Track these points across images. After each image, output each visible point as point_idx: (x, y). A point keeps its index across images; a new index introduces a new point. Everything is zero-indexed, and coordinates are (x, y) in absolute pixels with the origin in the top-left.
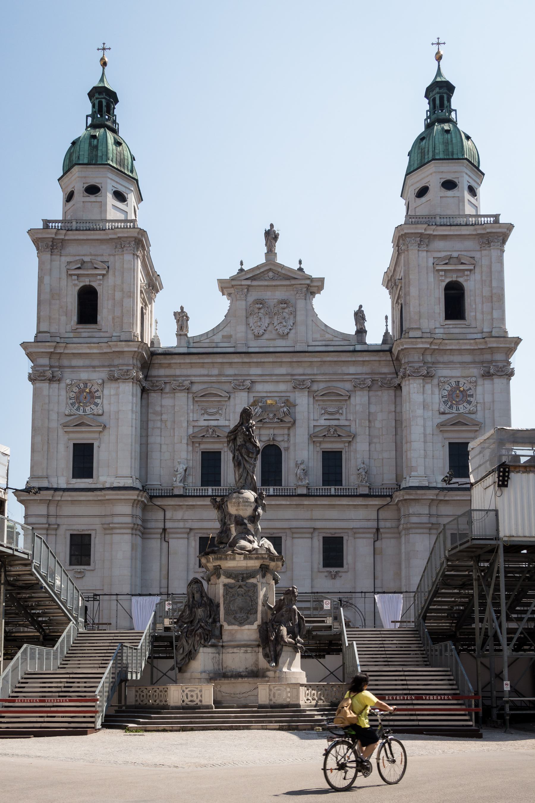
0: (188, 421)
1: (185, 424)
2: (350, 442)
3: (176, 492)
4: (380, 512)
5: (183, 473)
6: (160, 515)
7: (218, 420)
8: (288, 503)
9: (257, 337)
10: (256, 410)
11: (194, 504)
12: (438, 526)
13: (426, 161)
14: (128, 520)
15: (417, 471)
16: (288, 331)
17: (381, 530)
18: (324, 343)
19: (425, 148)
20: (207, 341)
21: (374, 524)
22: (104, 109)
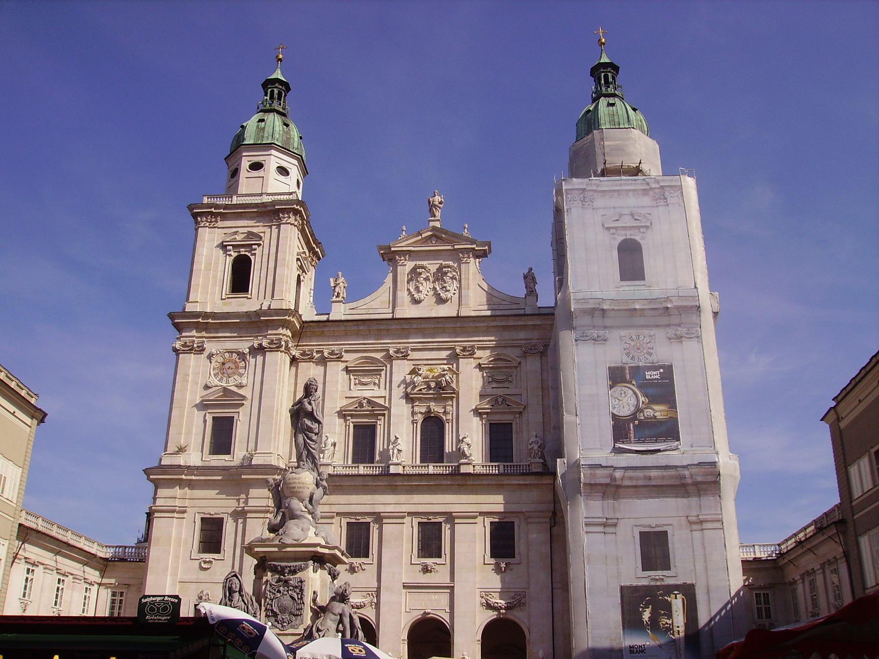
2: (521, 413)
7: (373, 390)
8: (449, 483)
9: (416, 302)
10: (415, 379)
11: (342, 484)
16: (452, 295)
19: (591, 119)
22: (276, 96)
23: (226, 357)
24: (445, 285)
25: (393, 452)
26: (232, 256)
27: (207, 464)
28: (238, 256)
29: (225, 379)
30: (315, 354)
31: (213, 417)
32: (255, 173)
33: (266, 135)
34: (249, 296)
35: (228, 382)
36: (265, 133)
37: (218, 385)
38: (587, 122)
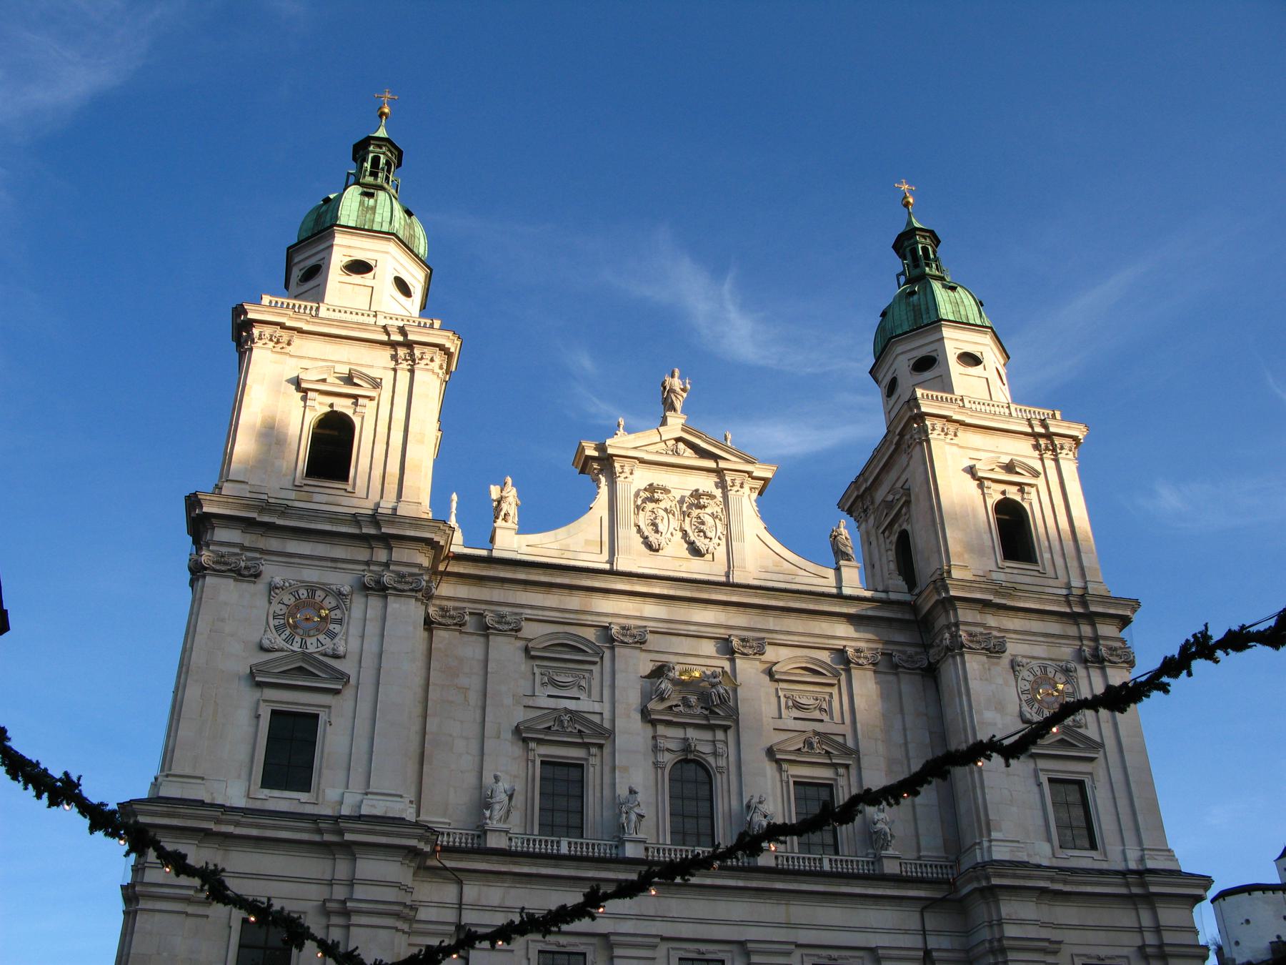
0: (513, 696)
1: (508, 701)
3: (493, 842)
4: (926, 915)
5: (507, 798)
6: (448, 892)
7: (579, 699)
8: (741, 883)
10: (663, 686)
12: (1056, 946)
13: (925, 322)
14: (390, 894)
15: (1000, 830)
17: (934, 954)
18: (781, 577)
19: (920, 305)
20: (555, 546)
21: (916, 941)
23: (301, 597)
24: (702, 527)
25: (629, 821)
26: (315, 410)
27: (257, 805)
28: (331, 411)
29: (298, 639)
30: (467, 618)
31: (272, 710)
32: (356, 278)
33: (378, 219)
34: (350, 489)
35: (303, 644)
36: (377, 215)
37: (286, 649)
38: (912, 308)
